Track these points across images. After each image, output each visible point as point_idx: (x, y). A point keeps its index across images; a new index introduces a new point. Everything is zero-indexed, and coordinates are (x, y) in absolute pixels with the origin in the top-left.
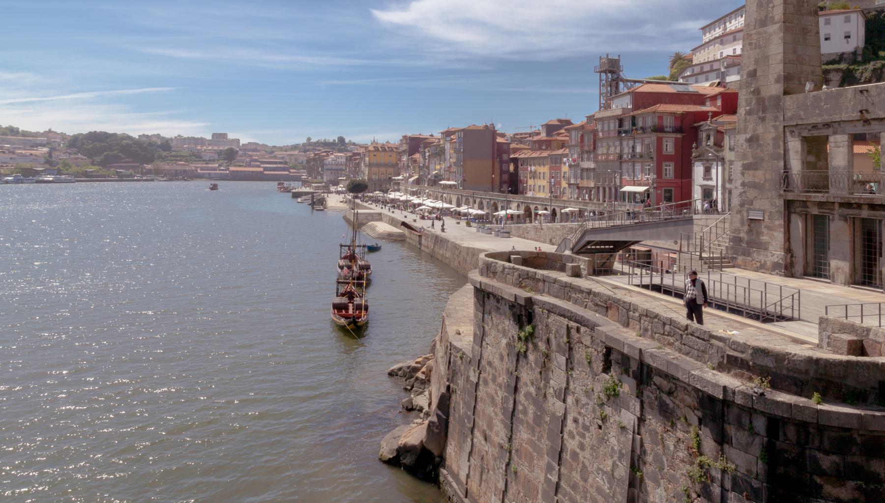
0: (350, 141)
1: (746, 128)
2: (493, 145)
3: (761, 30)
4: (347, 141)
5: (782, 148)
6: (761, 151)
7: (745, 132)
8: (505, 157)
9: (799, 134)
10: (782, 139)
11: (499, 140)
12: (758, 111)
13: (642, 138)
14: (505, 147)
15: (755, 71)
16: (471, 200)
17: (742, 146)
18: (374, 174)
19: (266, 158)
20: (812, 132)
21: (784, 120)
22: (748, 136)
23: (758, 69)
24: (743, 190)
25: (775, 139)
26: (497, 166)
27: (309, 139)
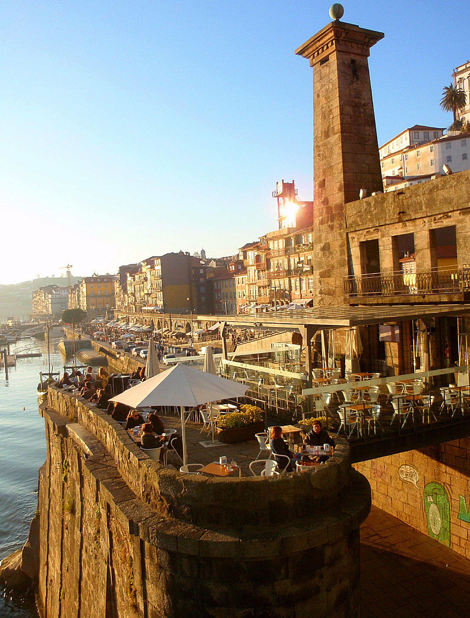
5: (346, 254)
6: (332, 259)
9: (358, 239)
14: (202, 271)
20: (367, 237)
21: (346, 228)
24: (320, 298)
25: (341, 246)
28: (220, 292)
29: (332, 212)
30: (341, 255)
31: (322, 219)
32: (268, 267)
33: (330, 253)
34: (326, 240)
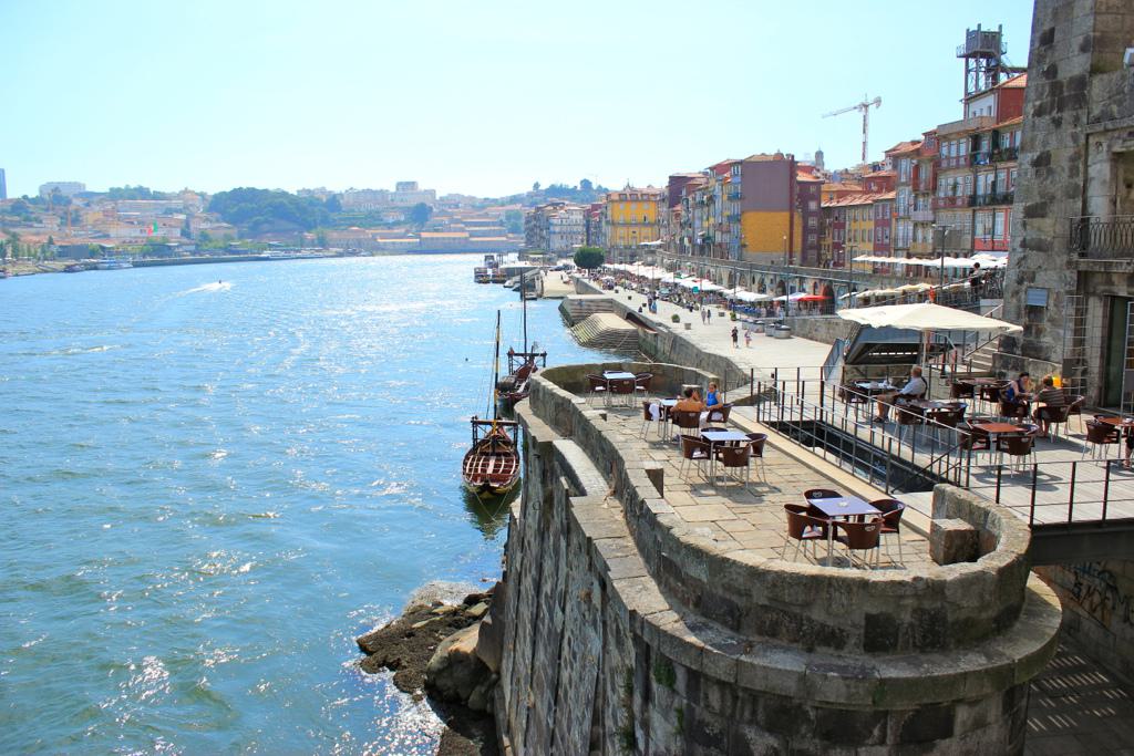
0: (600, 186)
2: (791, 188)
4: (594, 187)
5: (1081, 175)
6: (1052, 182)
8: (813, 206)
9: (1109, 146)
10: (1083, 159)
11: (802, 177)
13: (1008, 168)
14: (813, 189)
16: (748, 277)
17: (1026, 174)
18: (620, 238)
19: (472, 218)
20: (1129, 143)
22: (1036, 155)
24: (1022, 255)
26: (798, 220)
27: (536, 186)
28: (844, 228)
29: (1062, 92)
30: (1071, 176)
31: (1041, 106)
32: (935, 189)
33: (1051, 172)
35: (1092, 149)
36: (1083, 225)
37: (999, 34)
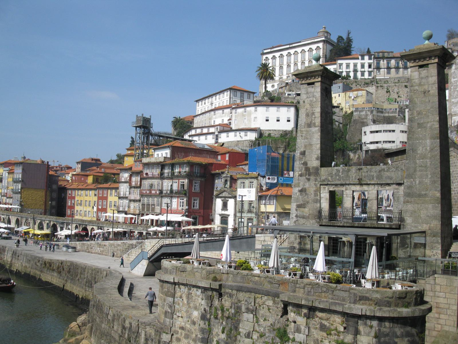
1: (299, 183)
3: (308, 129)
5: (319, 196)
7: (299, 186)
9: (328, 189)
12: (306, 175)
15: (304, 152)
17: (296, 194)
20: (335, 188)
22: (300, 189)
23: (306, 151)
30: (315, 196)
34: (304, 186)
35: (321, 189)
36: (320, 212)
37: (150, 119)
